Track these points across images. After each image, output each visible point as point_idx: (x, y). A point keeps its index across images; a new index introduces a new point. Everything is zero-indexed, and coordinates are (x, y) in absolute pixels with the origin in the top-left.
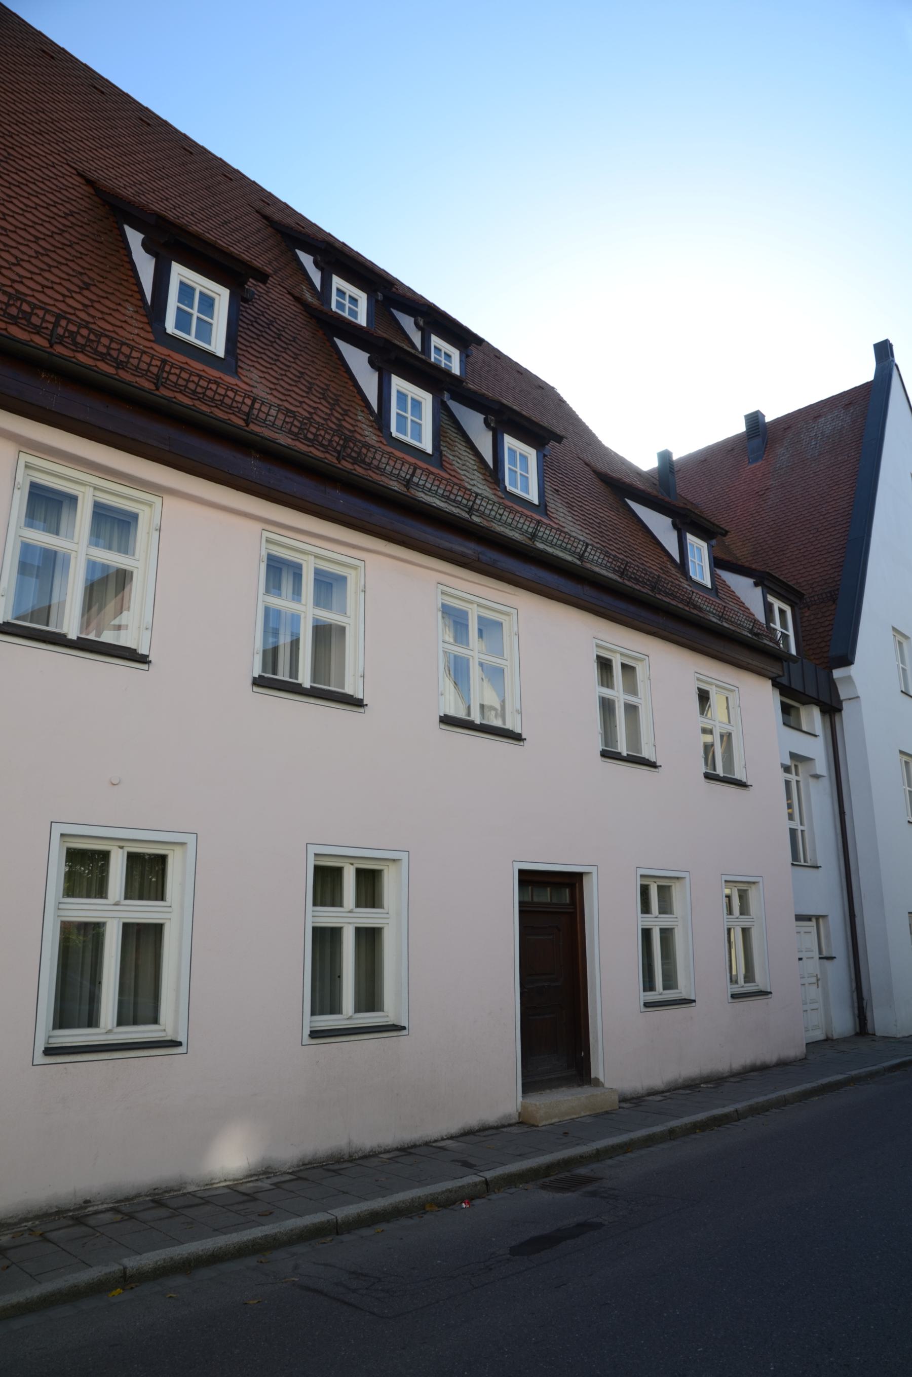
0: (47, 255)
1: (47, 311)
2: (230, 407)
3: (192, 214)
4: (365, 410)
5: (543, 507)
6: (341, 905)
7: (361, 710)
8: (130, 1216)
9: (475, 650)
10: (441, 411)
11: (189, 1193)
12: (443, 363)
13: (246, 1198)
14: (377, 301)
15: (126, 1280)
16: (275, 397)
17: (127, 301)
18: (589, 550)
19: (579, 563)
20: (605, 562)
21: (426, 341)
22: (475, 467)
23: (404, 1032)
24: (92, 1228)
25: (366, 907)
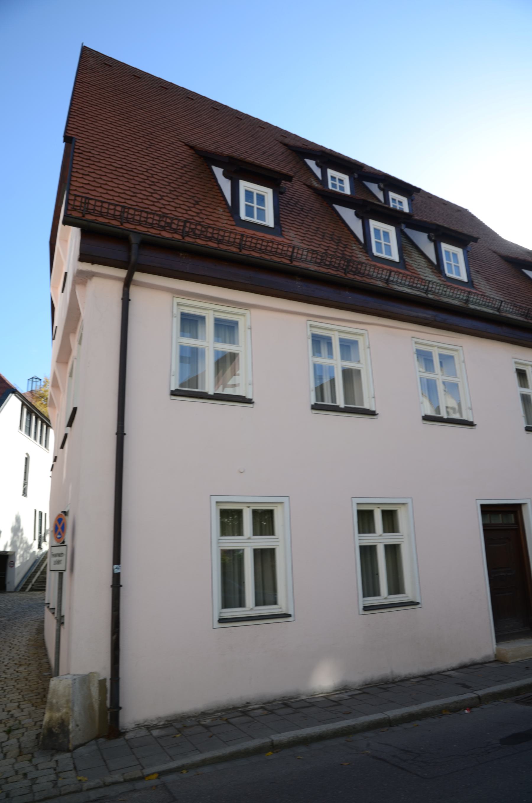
0: (175, 191)
1: (179, 220)
2: (281, 254)
3: (246, 152)
4: (356, 242)
5: (470, 283)
6: (374, 532)
7: (375, 417)
8: (272, 712)
9: (439, 376)
10: (401, 236)
11: (302, 700)
12: (398, 207)
13: (334, 703)
14: (355, 179)
15: (274, 747)
16: (305, 244)
17: (218, 206)
18: (503, 305)
19: (497, 313)
20: (514, 311)
21: (386, 197)
22: (426, 266)
23: (419, 606)
24: (252, 717)
25: (389, 532)
